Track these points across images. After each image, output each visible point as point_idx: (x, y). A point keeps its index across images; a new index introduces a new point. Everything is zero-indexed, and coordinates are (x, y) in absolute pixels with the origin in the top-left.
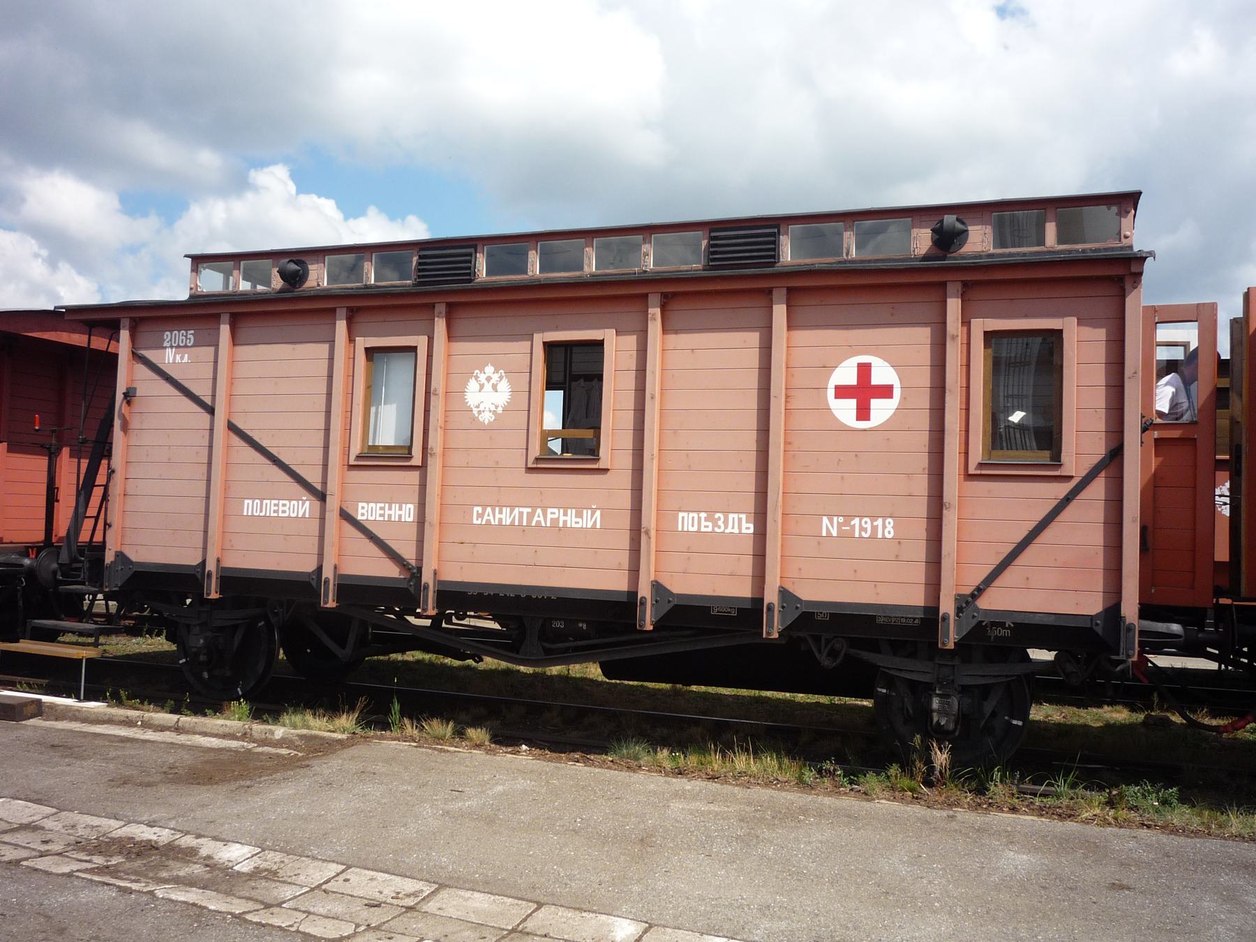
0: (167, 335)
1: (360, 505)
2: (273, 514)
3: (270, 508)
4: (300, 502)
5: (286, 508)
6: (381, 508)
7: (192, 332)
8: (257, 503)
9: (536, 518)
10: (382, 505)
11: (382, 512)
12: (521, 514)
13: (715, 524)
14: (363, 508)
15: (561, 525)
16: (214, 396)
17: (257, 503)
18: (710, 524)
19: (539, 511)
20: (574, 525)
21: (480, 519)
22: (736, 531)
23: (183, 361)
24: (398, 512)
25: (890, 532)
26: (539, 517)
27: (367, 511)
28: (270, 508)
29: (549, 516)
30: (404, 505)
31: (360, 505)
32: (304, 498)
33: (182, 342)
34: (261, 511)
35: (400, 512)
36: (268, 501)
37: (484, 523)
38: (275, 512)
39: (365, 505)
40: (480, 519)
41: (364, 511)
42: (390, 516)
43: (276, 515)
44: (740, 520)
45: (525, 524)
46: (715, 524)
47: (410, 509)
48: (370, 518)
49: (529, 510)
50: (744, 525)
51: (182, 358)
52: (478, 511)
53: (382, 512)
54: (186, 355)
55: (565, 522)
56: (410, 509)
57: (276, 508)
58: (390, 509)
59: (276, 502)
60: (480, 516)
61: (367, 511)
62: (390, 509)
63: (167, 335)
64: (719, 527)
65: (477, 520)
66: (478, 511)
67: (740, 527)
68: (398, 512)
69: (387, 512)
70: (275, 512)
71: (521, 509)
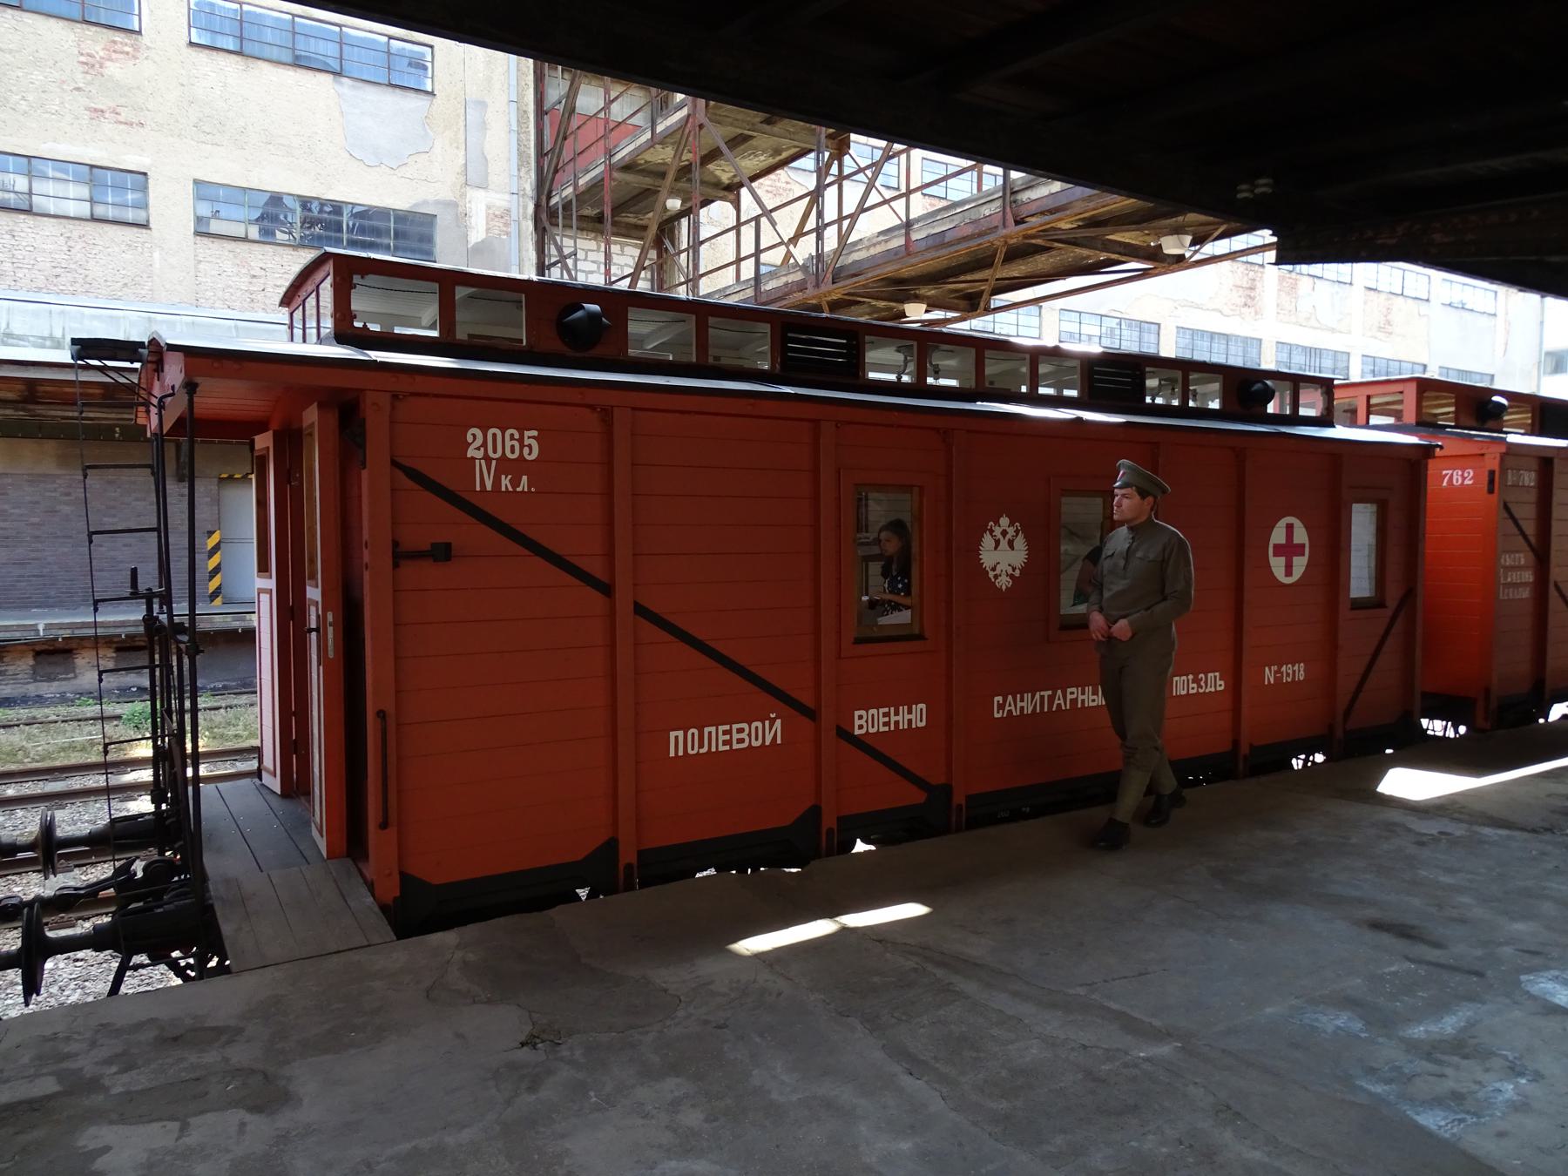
0: (474, 436)
1: (857, 713)
2: (721, 748)
3: (717, 738)
4: (767, 723)
5: (744, 735)
6: (885, 715)
7: (535, 433)
8: (693, 734)
9: (1056, 702)
10: (886, 710)
11: (887, 719)
12: (1042, 697)
13: (1200, 686)
14: (861, 717)
15: (1079, 706)
16: (610, 556)
17: (693, 734)
18: (1195, 685)
19: (1059, 692)
20: (1091, 704)
21: (1001, 711)
22: (1213, 690)
23: (519, 489)
24: (907, 717)
25: (1301, 676)
26: (1059, 699)
27: (867, 722)
28: (717, 738)
29: (1069, 697)
30: (914, 706)
31: (857, 713)
32: (773, 716)
33: (513, 451)
34: (701, 745)
35: (910, 717)
36: (713, 729)
37: (1005, 715)
38: (725, 743)
39: (863, 713)
40: (1001, 711)
41: (863, 722)
42: (897, 723)
43: (727, 748)
44: (1215, 677)
45: (1046, 710)
46: (1200, 686)
47: (921, 710)
48: (871, 731)
49: (1050, 692)
50: (1219, 682)
51: (515, 483)
52: (998, 701)
53: (887, 719)
54: (525, 478)
55: (1083, 701)
56: (921, 710)
57: (727, 737)
58: (897, 714)
59: (727, 727)
60: (1001, 707)
61: (867, 722)
62: (897, 714)
63: (474, 436)
64: (1202, 688)
65: (998, 713)
66: (998, 701)
67: (1215, 686)
68: (907, 717)
69: (893, 718)
70: (725, 743)
71: (1042, 693)
